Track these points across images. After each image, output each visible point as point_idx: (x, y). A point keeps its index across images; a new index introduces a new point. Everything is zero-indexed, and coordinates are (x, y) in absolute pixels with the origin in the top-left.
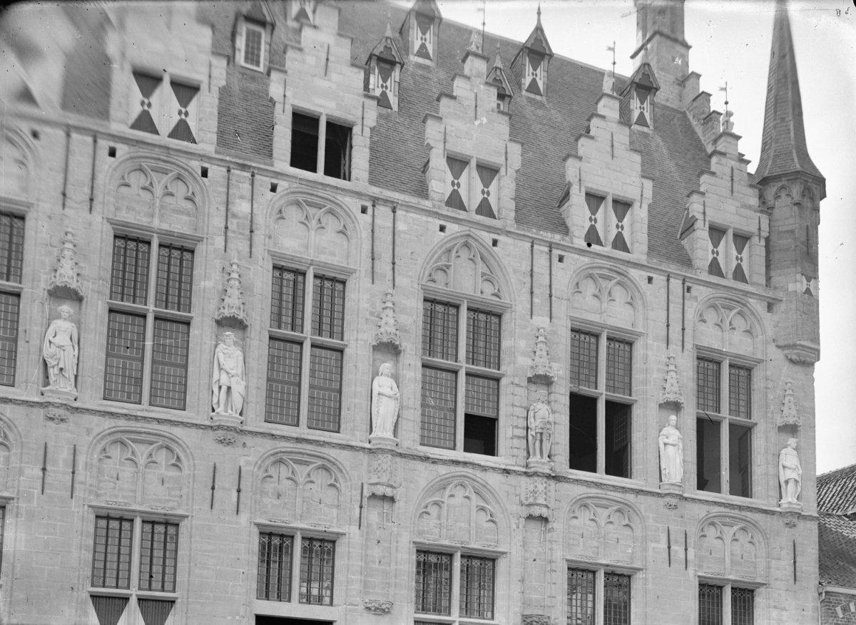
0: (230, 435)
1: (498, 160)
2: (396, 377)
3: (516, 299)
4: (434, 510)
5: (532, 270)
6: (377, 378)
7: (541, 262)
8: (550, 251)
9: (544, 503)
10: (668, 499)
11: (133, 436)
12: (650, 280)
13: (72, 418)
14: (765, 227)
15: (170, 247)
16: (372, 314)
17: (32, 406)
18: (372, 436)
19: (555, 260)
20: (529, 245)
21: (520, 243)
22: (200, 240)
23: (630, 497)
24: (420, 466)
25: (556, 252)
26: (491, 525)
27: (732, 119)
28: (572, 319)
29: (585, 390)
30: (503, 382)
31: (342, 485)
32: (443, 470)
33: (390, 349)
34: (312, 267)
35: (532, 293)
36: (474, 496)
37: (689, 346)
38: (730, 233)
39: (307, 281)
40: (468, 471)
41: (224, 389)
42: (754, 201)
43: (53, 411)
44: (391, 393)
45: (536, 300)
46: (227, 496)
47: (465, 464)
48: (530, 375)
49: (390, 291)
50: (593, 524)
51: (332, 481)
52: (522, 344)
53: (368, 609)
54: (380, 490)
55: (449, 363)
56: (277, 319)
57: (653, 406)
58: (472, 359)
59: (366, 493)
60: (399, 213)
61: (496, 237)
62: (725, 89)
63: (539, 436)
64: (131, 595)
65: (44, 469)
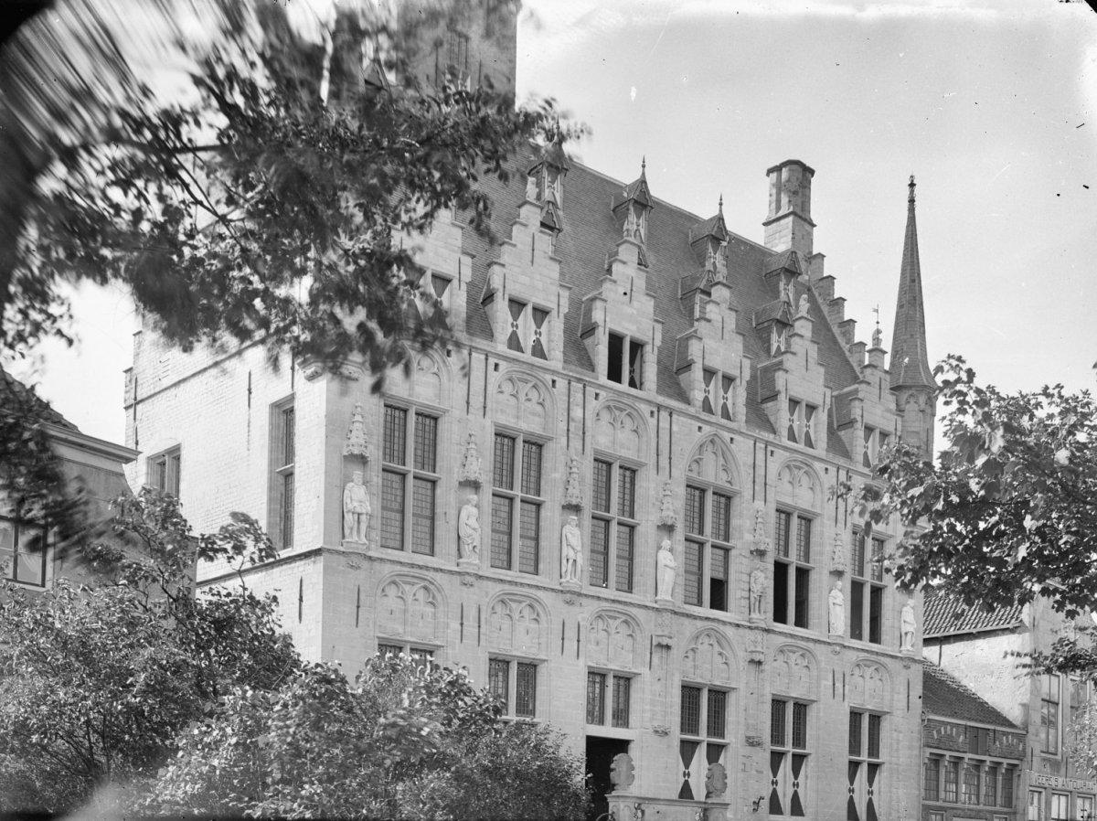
0: (574, 597)
1: (734, 372)
3: (743, 485)
4: (691, 654)
13: (477, 583)
14: (899, 427)
16: (657, 499)
19: (769, 454)
22: (550, 439)
23: (811, 645)
24: (686, 621)
25: (770, 448)
26: (725, 666)
27: (881, 336)
29: (783, 559)
30: (733, 553)
31: (638, 636)
32: (699, 624)
33: (668, 529)
36: (716, 645)
37: (849, 525)
38: (877, 432)
40: (714, 625)
41: (571, 561)
42: (893, 406)
43: (469, 579)
46: (571, 645)
50: (785, 665)
52: (748, 524)
53: (656, 732)
56: (597, 505)
57: (826, 572)
59: (654, 643)
60: (674, 416)
61: (733, 436)
62: (877, 311)
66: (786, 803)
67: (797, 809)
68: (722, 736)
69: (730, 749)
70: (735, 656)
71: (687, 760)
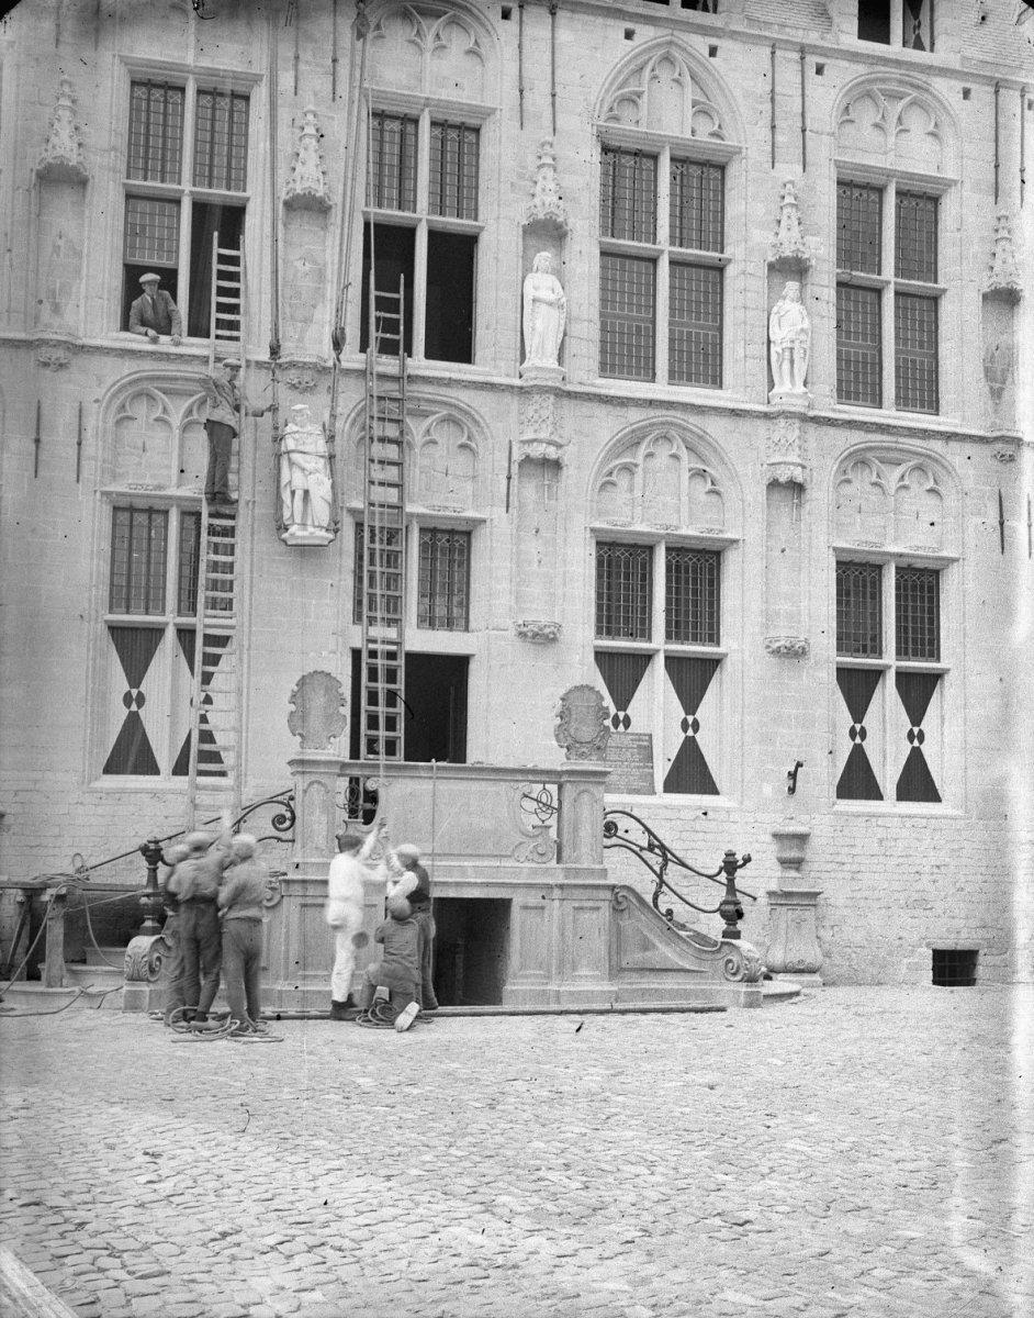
0: (307, 376)
2: (558, 273)
3: (746, 135)
5: (773, 91)
6: (530, 275)
7: (788, 75)
8: (802, 58)
9: (799, 461)
10: (999, 446)
11: (166, 385)
12: (966, 94)
15: (215, 93)
16: (521, 176)
17: (18, 347)
18: (525, 365)
20: (769, 50)
21: (755, 49)
23: (937, 446)
24: (600, 411)
25: (812, 60)
26: (714, 498)
28: (839, 165)
30: (730, 271)
31: (479, 444)
32: (635, 416)
34: (427, 110)
35: (773, 127)
36: (684, 453)
39: (420, 132)
40: (676, 416)
44: (552, 297)
45: (780, 138)
47: (670, 405)
48: (771, 259)
49: (549, 138)
50: (877, 490)
51: (464, 440)
52: (759, 210)
54: (537, 451)
55: (643, 246)
57: (973, 300)
58: (678, 237)
59: (517, 456)
61: (714, 41)
63: (787, 353)
64: (167, 624)
65: (37, 441)
66: (888, 774)
67: (918, 783)
68: (714, 638)
69: (728, 665)
70: (734, 477)
71: (858, 708)
